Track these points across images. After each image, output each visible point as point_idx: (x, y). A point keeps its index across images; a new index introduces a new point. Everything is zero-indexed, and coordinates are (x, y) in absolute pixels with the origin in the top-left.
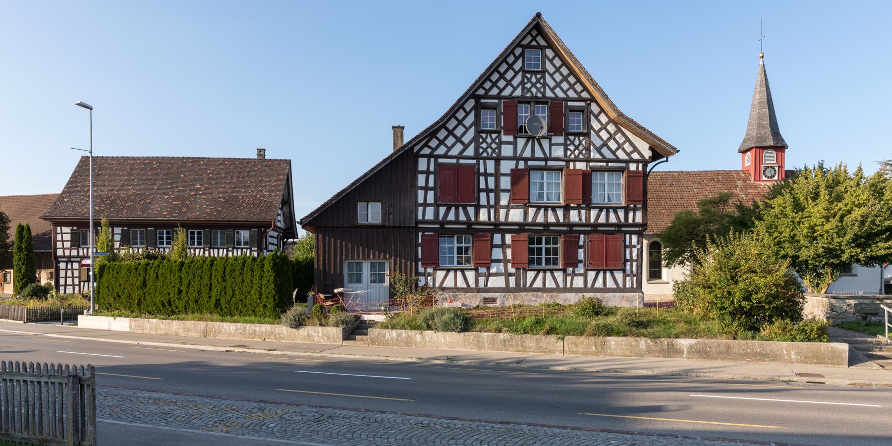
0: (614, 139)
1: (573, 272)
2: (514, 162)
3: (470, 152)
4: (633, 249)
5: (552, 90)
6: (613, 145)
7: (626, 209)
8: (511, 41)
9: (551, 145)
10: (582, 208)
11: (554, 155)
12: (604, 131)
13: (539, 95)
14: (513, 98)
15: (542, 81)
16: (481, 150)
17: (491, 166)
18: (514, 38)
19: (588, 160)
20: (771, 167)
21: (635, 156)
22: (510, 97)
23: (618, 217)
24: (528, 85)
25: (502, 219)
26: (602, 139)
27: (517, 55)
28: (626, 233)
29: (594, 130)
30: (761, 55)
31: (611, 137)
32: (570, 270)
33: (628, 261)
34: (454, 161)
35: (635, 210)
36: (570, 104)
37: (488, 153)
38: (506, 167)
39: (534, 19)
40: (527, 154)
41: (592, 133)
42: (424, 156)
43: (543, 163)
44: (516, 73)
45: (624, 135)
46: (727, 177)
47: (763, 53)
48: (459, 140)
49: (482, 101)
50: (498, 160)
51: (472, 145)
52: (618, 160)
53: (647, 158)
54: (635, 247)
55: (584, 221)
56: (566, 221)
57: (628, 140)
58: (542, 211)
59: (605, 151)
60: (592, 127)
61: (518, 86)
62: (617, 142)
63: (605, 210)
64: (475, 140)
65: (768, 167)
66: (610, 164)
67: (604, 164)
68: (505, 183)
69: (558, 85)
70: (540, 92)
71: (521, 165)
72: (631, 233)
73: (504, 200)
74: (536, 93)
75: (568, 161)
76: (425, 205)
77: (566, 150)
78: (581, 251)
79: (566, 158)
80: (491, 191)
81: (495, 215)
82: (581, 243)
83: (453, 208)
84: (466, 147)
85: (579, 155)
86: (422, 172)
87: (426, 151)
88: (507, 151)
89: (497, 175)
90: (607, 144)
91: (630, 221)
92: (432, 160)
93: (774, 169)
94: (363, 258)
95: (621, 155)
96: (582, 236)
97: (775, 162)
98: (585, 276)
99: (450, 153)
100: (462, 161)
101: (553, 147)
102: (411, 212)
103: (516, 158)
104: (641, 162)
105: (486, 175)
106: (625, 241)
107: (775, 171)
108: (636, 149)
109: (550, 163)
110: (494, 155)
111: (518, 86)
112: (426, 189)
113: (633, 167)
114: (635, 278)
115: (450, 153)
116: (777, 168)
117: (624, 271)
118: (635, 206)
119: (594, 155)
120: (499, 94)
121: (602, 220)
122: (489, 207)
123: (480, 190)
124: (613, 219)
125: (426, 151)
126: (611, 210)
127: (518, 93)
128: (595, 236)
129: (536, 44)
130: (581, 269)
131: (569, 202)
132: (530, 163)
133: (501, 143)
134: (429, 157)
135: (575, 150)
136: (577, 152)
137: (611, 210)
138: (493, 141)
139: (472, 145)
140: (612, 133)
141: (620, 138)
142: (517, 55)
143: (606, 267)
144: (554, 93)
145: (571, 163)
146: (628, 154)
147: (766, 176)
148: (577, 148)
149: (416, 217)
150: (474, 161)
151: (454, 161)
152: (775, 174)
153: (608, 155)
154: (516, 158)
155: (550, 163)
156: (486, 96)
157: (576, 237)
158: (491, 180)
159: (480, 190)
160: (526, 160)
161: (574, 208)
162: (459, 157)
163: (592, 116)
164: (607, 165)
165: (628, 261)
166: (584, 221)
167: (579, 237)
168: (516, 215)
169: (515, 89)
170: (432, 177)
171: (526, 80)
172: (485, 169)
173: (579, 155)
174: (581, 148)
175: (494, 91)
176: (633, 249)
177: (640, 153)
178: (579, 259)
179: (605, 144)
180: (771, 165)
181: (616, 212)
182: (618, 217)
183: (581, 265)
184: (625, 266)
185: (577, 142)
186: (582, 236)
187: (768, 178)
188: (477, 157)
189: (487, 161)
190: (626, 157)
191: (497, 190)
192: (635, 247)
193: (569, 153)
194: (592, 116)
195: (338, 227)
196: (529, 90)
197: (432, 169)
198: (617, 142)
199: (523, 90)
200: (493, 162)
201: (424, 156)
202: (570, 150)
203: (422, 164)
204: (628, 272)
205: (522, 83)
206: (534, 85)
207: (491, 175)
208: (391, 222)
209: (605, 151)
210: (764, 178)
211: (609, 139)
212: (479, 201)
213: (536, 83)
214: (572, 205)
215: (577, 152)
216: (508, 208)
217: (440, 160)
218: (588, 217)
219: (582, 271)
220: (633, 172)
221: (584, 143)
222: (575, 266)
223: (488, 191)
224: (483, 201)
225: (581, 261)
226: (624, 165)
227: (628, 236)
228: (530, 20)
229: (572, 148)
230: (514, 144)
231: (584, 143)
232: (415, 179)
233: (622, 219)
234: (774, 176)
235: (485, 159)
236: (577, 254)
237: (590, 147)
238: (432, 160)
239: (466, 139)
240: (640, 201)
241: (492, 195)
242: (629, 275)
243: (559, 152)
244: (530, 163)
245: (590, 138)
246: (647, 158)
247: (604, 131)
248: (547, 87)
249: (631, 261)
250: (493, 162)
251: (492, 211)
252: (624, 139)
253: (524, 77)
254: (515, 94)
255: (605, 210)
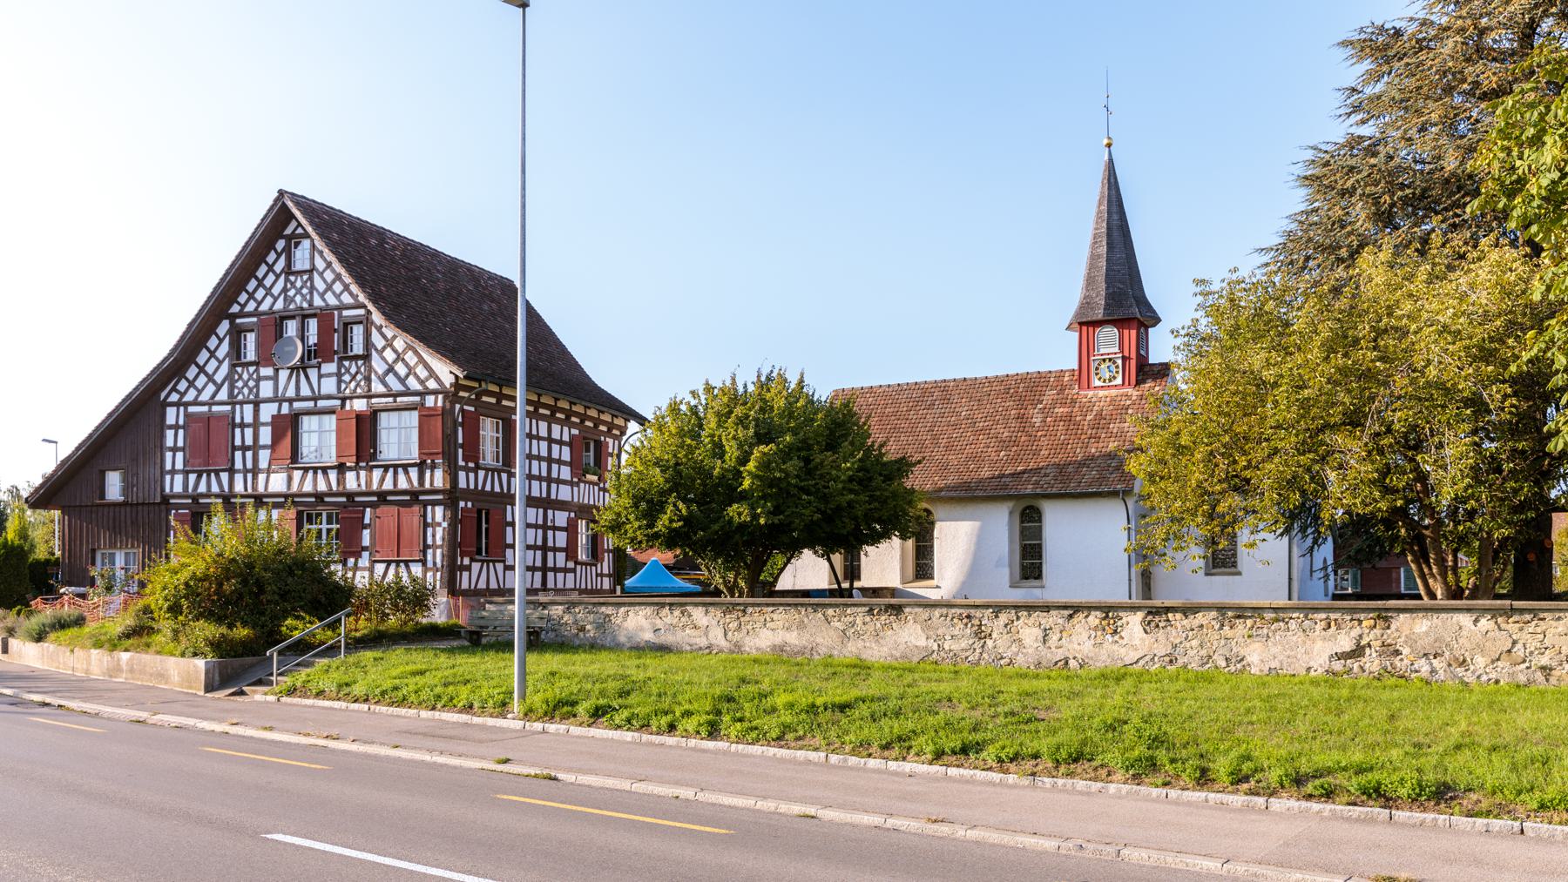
0: (403, 360)
1: (356, 563)
2: (277, 404)
3: (223, 395)
4: (437, 528)
5: (322, 296)
6: (401, 369)
7: (421, 466)
8: (249, 235)
9: (320, 376)
10: (361, 468)
11: (324, 391)
12: (389, 349)
13: (305, 305)
14: (273, 313)
15: (308, 284)
16: (236, 391)
17: (248, 410)
18: (252, 230)
19: (369, 396)
20: (1110, 360)
21: (432, 385)
22: (271, 312)
23: (409, 480)
24: (292, 293)
25: (261, 489)
26: (386, 362)
27: (279, 250)
28: (425, 504)
29: (376, 349)
30: (1106, 141)
31: (399, 357)
32: (351, 561)
33: (429, 547)
34: (205, 409)
35: (433, 467)
36: (346, 313)
37: (244, 395)
38: (268, 412)
39: (276, 201)
40: (291, 393)
41: (374, 353)
42: (172, 404)
43: (311, 404)
44: (278, 276)
45: (416, 353)
46: (1026, 389)
47: (1109, 138)
48: (210, 379)
49: (238, 321)
50: (257, 404)
51: (226, 385)
52: (408, 393)
53: (448, 386)
54: (439, 524)
55: (364, 487)
56: (341, 488)
57: (421, 360)
58: (310, 474)
59: (390, 379)
60: (373, 345)
61: (280, 295)
62: (407, 365)
63: (391, 470)
64: (230, 378)
65: (1104, 360)
66: (399, 399)
67: (391, 399)
68: (266, 436)
69: (329, 287)
70: (305, 299)
71: (285, 409)
72: (434, 503)
73: (264, 456)
74: (301, 303)
75: (344, 400)
76: (173, 472)
77: (340, 382)
78: (366, 533)
79: (341, 395)
80: (248, 448)
81: (253, 483)
82: (367, 521)
83: (205, 475)
84: (219, 387)
85: (356, 389)
86: (170, 427)
87: (174, 397)
88: (266, 390)
89: (256, 425)
90: (393, 369)
91: (427, 485)
92: (182, 408)
93: (1114, 363)
94: (115, 547)
95: (413, 384)
96: (368, 510)
97: (1117, 350)
98: (371, 570)
99: (200, 399)
100: (215, 408)
101: (322, 380)
102: (155, 482)
103: (277, 399)
104: (441, 393)
105: (243, 426)
106: (425, 516)
107: (1117, 367)
108: (432, 374)
109: (322, 404)
110: (251, 397)
111: (280, 295)
112: (174, 449)
113: (430, 401)
114: (439, 574)
115: (200, 399)
116: (1119, 362)
117: (424, 562)
118: (433, 461)
119: (377, 387)
120: (256, 309)
121: (202, 488)
122: (245, 471)
123: (234, 448)
124: (403, 484)
125: (174, 397)
126: (400, 470)
127: (279, 305)
128: (383, 509)
129: (302, 232)
130: (364, 561)
131: (424, 457)
132: (296, 405)
133: (259, 379)
134: (177, 404)
135: (350, 382)
136: (353, 384)
137: (319, 471)
138: (251, 376)
139: (226, 385)
140: (400, 351)
141: (410, 358)
142: (279, 250)
143: (398, 556)
144: (324, 300)
145: (348, 402)
146: (422, 382)
147: (1100, 379)
148: (354, 377)
149: (163, 489)
150: (228, 408)
151: (205, 409)
152: (1117, 372)
153: (396, 386)
154: (277, 399)
155: (322, 404)
156: (242, 315)
157: (358, 512)
158: (249, 432)
159: (234, 448)
160: (291, 401)
161: (350, 469)
162: (211, 403)
163: (373, 328)
164: (210, 410)
165: (429, 547)
166: (364, 487)
167: (363, 513)
168: (277, 483)
169: (276, 299)
170: (181, 432)
171: (289, 286)
172: (242, 418)
173: (356, 389)
174: (359, 377)
175: (251, 306)
176: (437, 528)
177: (438, 380)
178: (364, 544)
179: (391, 370)
180: (1110, 356)
181: (407, 473)
182: (409, 480)
183: (366, 554)
184: (425, 555)
185: (353, 370)
186: (368, 510)
187: (1104, 381)
188: (232, 402)
189: (245, 406)
190: (418, 387)
191: (256, 447)
192: (439, 524)
193: (343, 386)
194: (373, 328)
195: (81, 506)
196: (292, 300)
197: (181, 422)
198: (407, 365)
199: (285, 300)
200: (251, 406)
201: (172, 404)
202: (345, 382)
203: (171, 415)
204: (430, 564)
205: (285, 290)
206: (299, 291)
207: (248, 426)
208: (135, 498)
209: (390, 379)
210: (1098, 383)
211: (395, 361)
212: (233, 463)
213: (302, 288)
214: (348, 464)
215: (353, 384)
216: (269, 471)
217: (191, 409)
218: (369, 482)
219: (367, 565)
220: (429, 408)
221: (362, 369)
222: (358, 555)
223: (244, 448)
224: (238, 465)
225: (365, 549)
226: (417, 399)
227: (429, 508)
228: (271, 202)
229: (347, 378)
230: (275, 378)
231: (362, 369)
232: (162, 437)
233: (416, 483)
234: (1115, 378)
235: (242, 403)
236: (360, 538)
237: (370, 375)
238: (182, 408)
239: (219, 378)
240: (438, 454)
241: (249, 454)
242: (431, 569)
243: (329, 386)
244: (296, 405)
245: (370, 361)
246: (448, 386)
247: (389, 349)
248: (315, 293)
249: (434, 547)
250: (251, 406)
251: (250, 476)
252: (416, 359)
253: (287, 280)
254: (276, 308)
255: (391, 470)
